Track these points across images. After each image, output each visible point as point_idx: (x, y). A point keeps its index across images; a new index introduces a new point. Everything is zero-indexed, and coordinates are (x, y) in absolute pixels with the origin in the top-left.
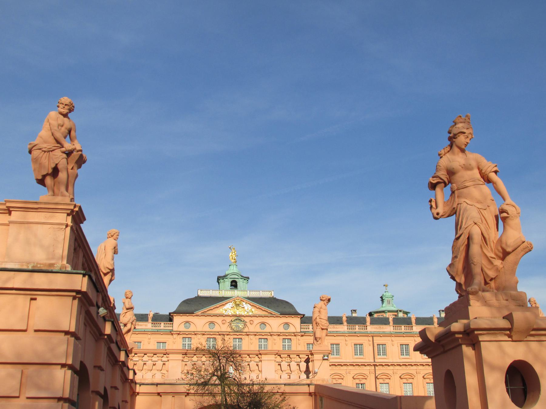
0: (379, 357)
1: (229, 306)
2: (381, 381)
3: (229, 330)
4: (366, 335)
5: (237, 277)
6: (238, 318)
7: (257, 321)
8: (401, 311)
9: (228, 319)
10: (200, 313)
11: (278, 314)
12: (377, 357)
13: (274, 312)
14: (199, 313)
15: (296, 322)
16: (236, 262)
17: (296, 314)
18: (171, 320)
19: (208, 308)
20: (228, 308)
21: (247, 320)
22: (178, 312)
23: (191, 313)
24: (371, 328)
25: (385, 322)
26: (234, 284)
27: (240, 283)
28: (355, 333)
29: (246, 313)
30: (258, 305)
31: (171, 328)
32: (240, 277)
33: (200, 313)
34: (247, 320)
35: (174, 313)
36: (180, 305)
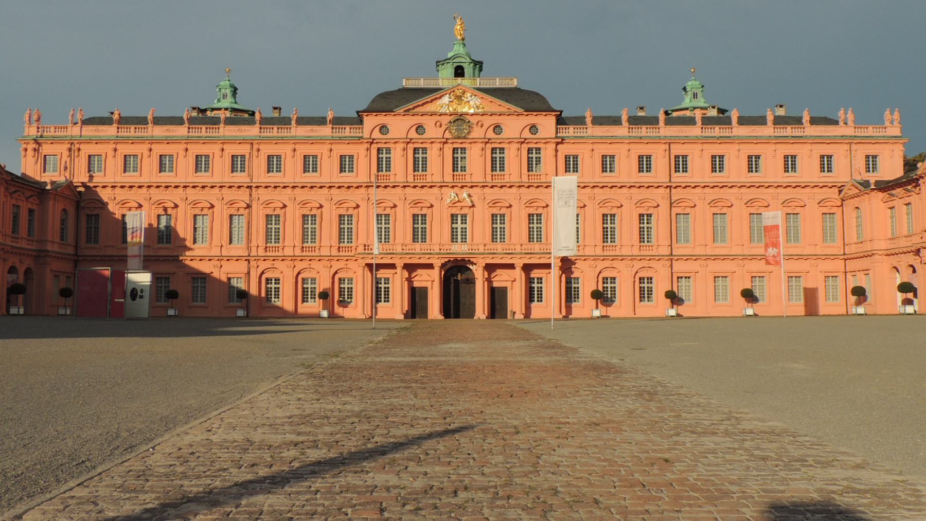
0: (677, 174)
1: (446, 99)
2: (679, 210)
3: (447, 135)
4: (657, 140)
5: (463, 60)
6: (460, 119)
7: (488, 121)
8: (714, 107)
9: (445, 120)
11: (520, 110)
12: (674, 174)
13: (514, 108)
14: (401, 110)
15: (546, 124)
16: (463, 39)
17: (548, 109)
18: (361, 122)
19: (415, 103)
20: (444, 104)
21: (474, 120)
22: (370, 111)
23: (388, 111)
24: (666, 131)
25: (691, 121)
26: (459, 72)
27: (468, 69)
28: (641, 138)
29: (472, 111)
30: (490, 98)
31: (361, 135)
32: (469, 60)
35: (364, 111)
36: (373, 101)
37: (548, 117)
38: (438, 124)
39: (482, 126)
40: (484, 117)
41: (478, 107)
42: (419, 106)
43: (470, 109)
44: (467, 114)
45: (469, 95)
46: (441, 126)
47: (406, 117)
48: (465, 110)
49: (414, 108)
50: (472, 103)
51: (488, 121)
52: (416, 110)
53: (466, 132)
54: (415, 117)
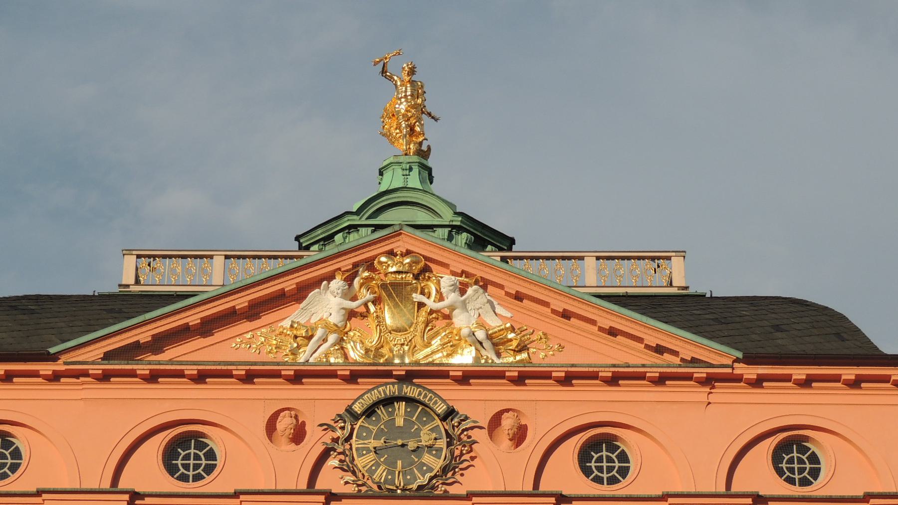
9: (322, 404)
10: (96, 352)
33: (96, 352)
34: (476, 403)
37: (868, 395)
38: (285, 424)
39: (519, 436)
40: (532, 392)
41: (497, 343)
42: (183, 333)
43: (454, 348)
44: (441, 374)
45: (447, 281)
46: (298, 435)
47: (116, 390)
48: (431, 353)
49: (159, 343)
50: (462, 321)
51: (551, 412)
52: (171, 353)
53: (437, 464)
54: (165, 390)
